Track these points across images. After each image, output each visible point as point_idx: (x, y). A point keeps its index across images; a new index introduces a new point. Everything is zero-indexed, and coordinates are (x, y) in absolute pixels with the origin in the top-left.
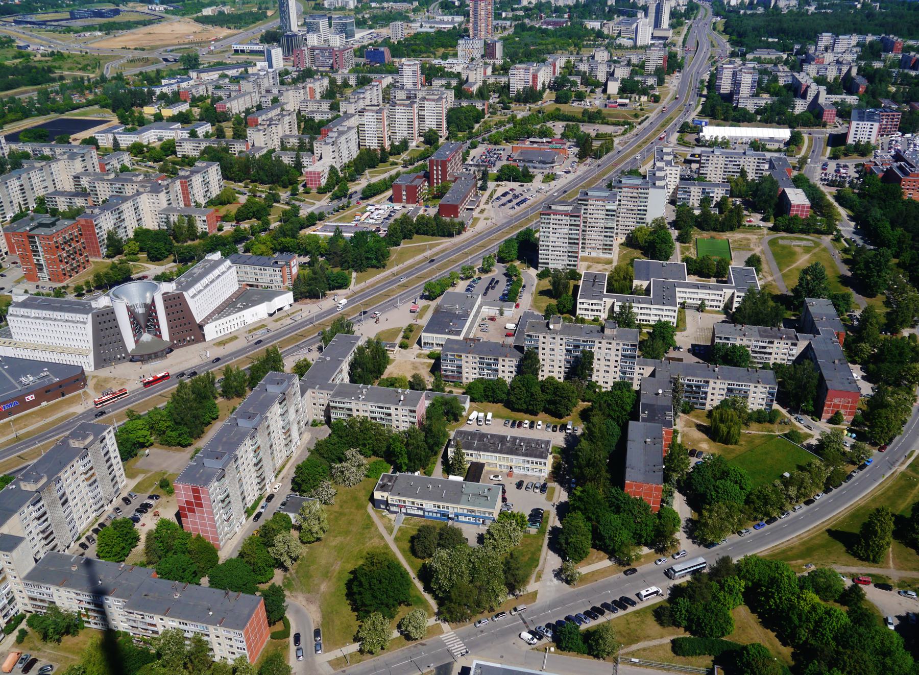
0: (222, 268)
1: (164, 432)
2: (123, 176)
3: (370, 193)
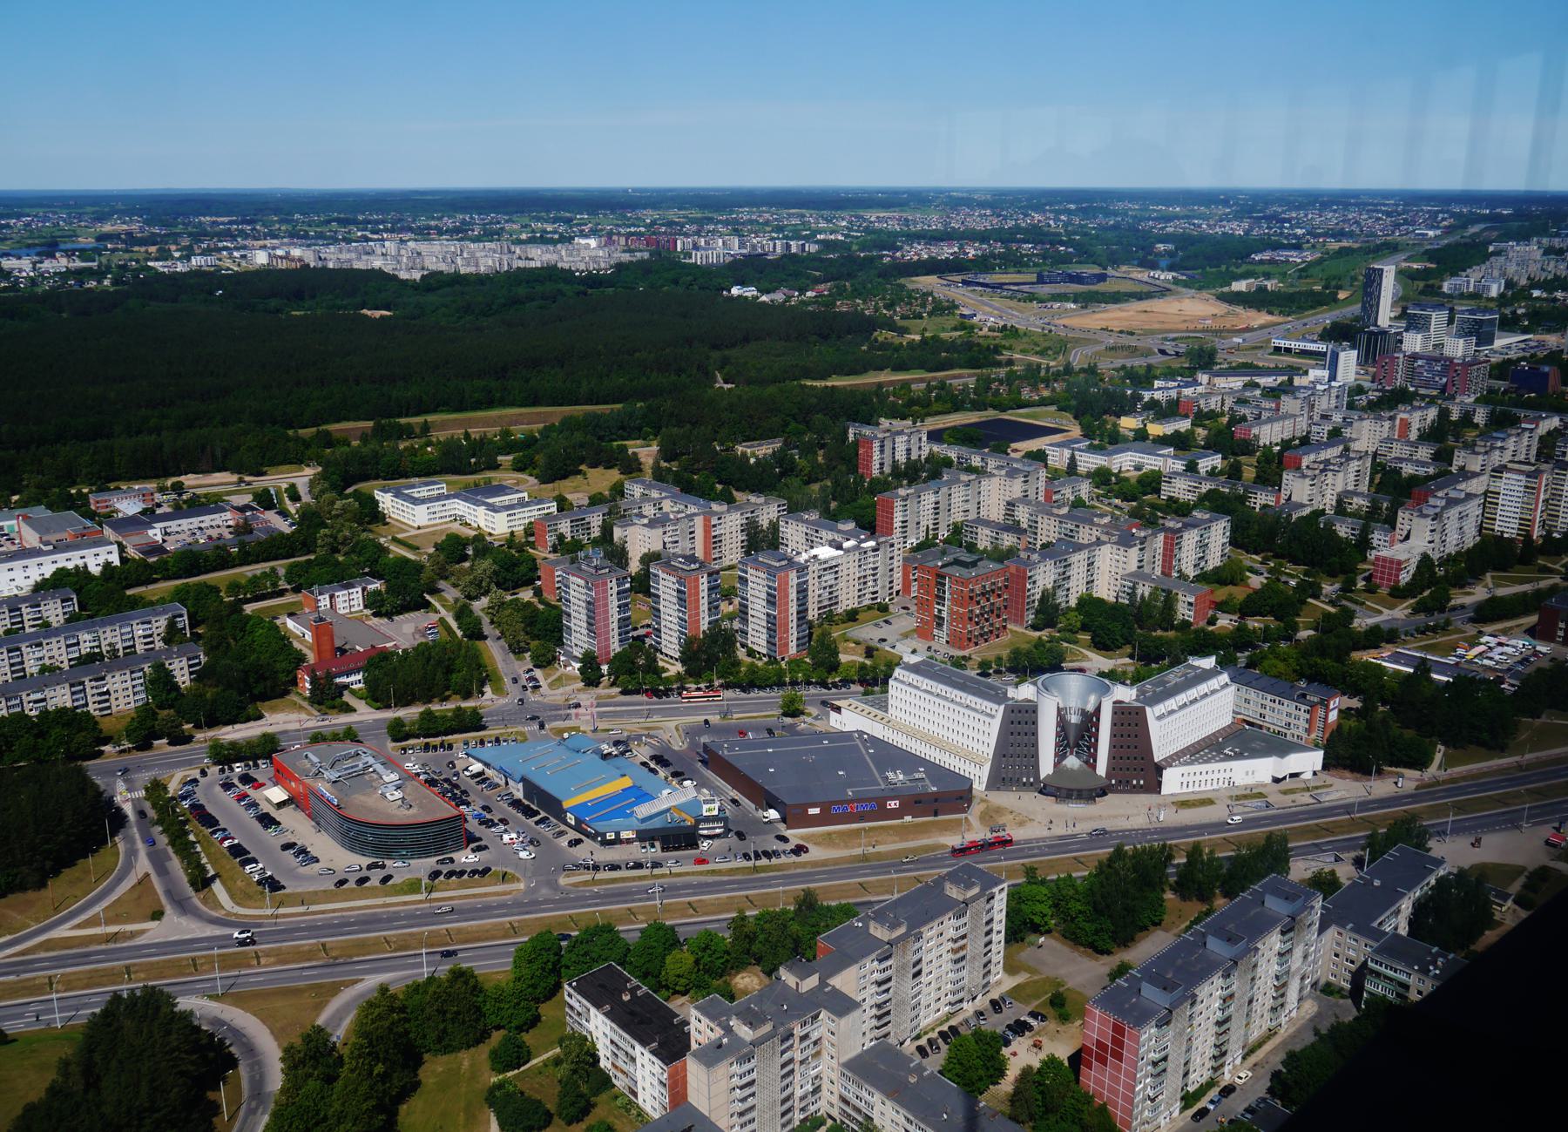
0: (1214, 683)
1: (1073, 919)
2: (1079, 512)
3: (1490, 613)
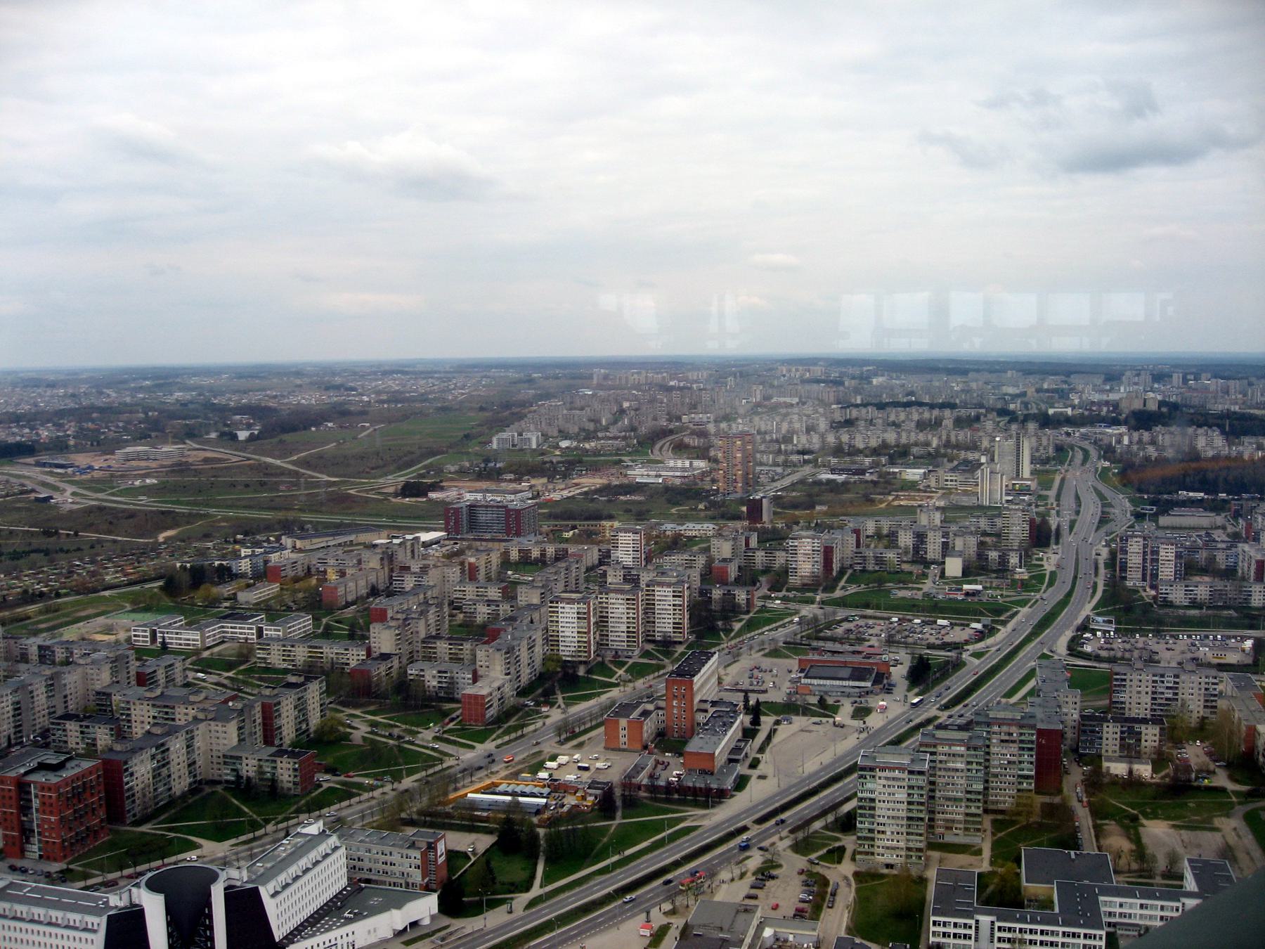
0: (323, 848)
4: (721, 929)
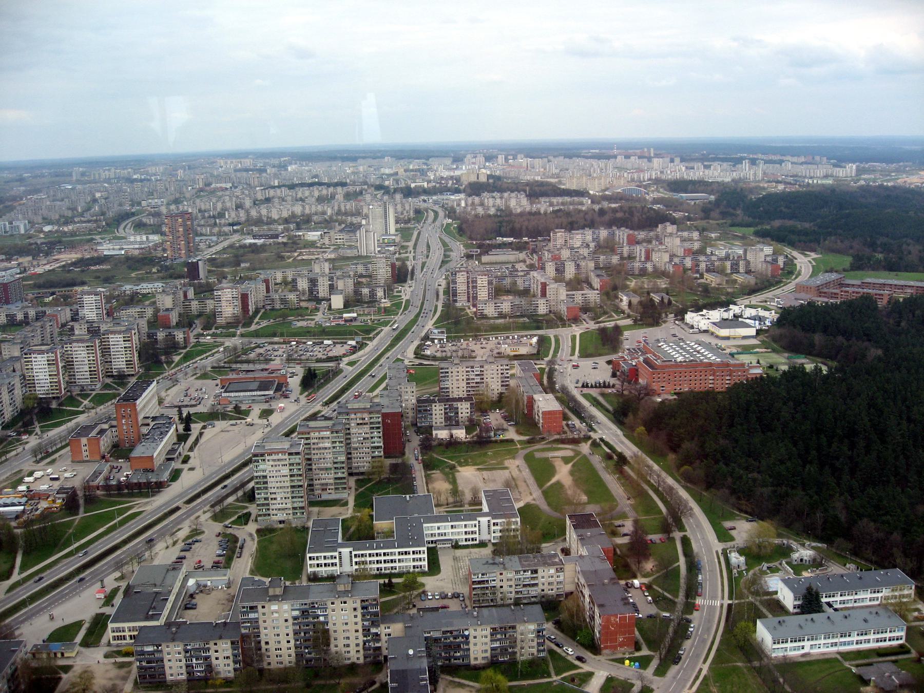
4: (155, 585)
